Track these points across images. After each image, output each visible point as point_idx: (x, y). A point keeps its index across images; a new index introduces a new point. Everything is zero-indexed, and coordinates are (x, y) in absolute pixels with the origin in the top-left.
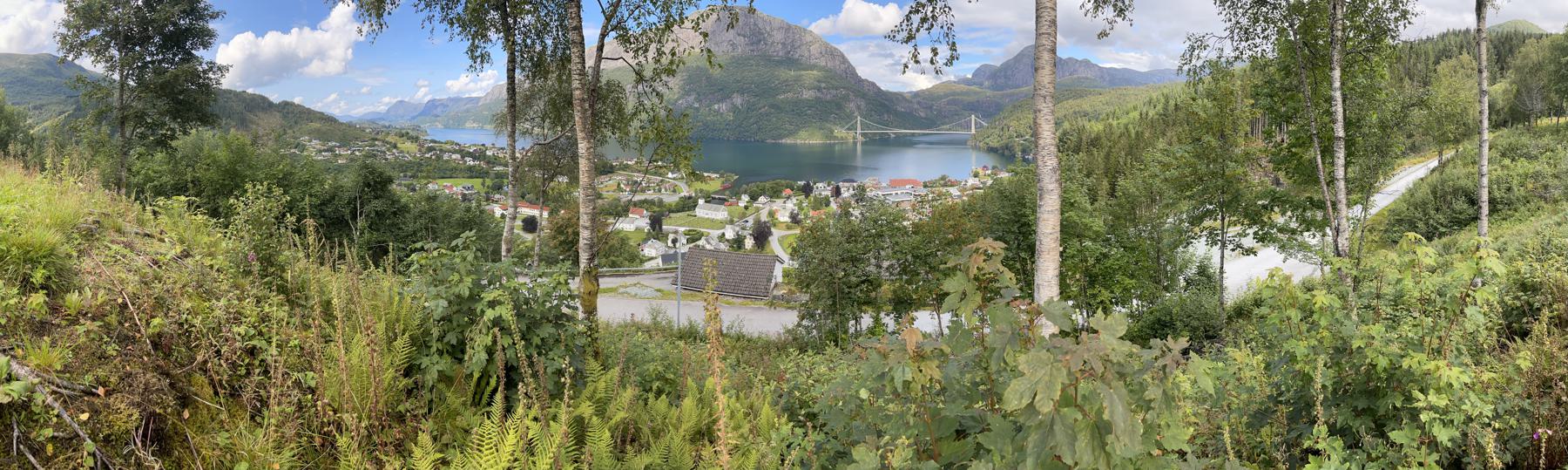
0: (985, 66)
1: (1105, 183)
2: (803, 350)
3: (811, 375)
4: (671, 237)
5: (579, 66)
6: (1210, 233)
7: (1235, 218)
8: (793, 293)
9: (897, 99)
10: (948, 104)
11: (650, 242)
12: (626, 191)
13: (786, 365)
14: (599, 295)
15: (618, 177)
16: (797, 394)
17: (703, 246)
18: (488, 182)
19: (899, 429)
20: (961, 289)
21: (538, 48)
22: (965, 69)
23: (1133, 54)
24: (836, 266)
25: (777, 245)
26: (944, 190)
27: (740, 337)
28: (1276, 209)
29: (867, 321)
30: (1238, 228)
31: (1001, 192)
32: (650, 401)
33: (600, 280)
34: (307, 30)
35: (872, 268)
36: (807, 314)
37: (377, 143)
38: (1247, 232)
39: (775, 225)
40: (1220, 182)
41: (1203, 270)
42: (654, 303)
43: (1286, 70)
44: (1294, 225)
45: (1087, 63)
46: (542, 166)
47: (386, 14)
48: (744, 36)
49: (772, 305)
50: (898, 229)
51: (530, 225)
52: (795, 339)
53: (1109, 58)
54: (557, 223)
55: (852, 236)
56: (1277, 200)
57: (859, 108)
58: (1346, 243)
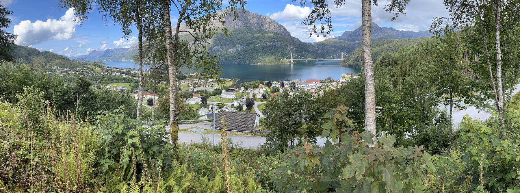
0: (347, 31)
1: (401, 78)
2: (267, 155)
3: (271, 165)
4: (211, 106)
5: (169, 35)
6: (446, 100)
7: (456, 94)
8: (264, 129)
9: (309, 46)
10: (331, 48)
11: (202, 109)
12: (191, 87)
13: (260, 161)
14: (179, 132)
15: (188, 81)
16: (265, 174)
17: (225, 110)
18: (132, 84)
19: (303, 187)
20: (330, 128)
21: (151, 27)
22: (337, 33)
23: (411, 25)
24: (282, 117)
25: (256, 108)
26: (329, 84)
27: (241, 150)
28: (474, 90)
29: (296, 141)
30: (457, 98)
31: (354, 84)
32: (201, 178)
33: (179, 126)
34: (54, 20)
35: (298, 118)
36: (270, 139)
37: (85, 68)
38: (461, 100)
39: (255, 100)
40: (450, 78)
41: (443, 116)
42: (204, 135)
43: (479, 31)
44: (482, 96)
45: (392, 29)
46: (154, 77)
47: (86, 13)
48: (241, 21)
49: (254, 135)
50: (309, 101)
51: (150, 102)
52: (265, 150)
53: (400, 27)
54: (162, 101)
55: (289, 104)
56: (474, 86)
57: (291, 49)
58: (502, 105)
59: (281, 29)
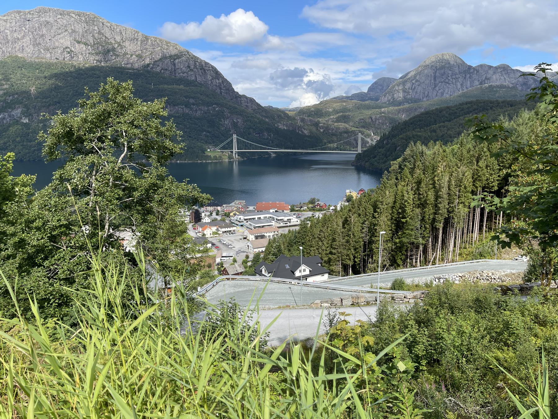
9: (279, 116)
45: (505, 69)
48: (86, 44)
59: (208, 72)
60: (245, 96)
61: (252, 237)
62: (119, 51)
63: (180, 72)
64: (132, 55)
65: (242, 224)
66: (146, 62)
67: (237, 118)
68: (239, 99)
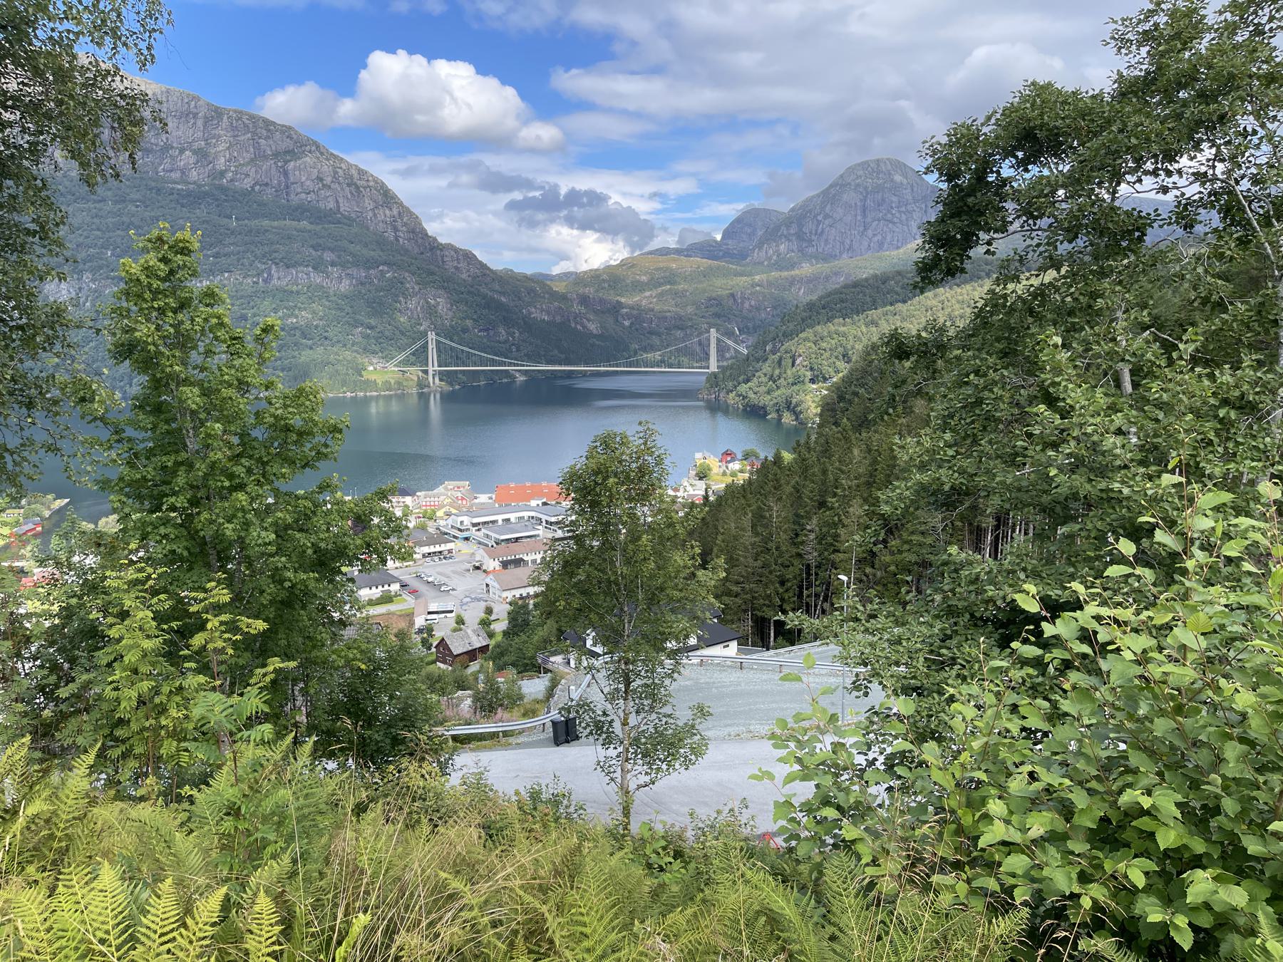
9: (531, 291)
59: (366, 193)
60: (452, 246)
61: (492, 565)
62: (153, 141)
63: (299, 190)
64: (182, 151)
65: (466, 534)
66: (217, 167)
67: (435, 297)
68: (438, 252)
